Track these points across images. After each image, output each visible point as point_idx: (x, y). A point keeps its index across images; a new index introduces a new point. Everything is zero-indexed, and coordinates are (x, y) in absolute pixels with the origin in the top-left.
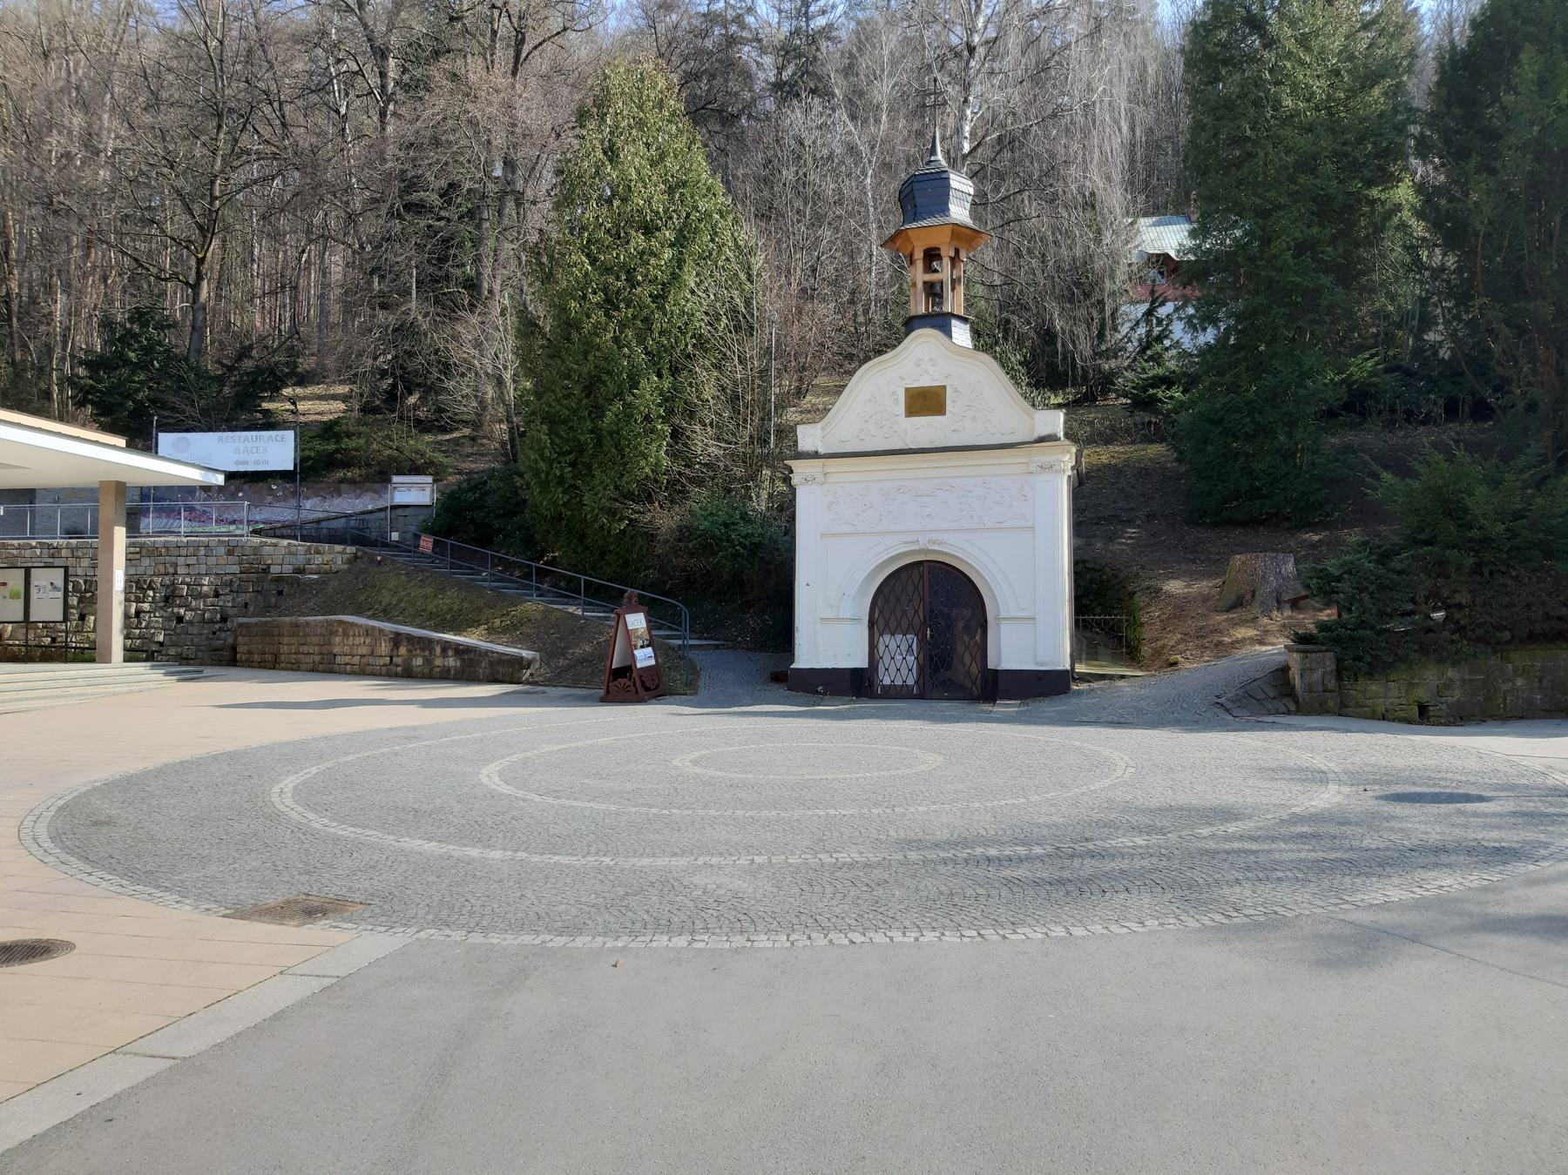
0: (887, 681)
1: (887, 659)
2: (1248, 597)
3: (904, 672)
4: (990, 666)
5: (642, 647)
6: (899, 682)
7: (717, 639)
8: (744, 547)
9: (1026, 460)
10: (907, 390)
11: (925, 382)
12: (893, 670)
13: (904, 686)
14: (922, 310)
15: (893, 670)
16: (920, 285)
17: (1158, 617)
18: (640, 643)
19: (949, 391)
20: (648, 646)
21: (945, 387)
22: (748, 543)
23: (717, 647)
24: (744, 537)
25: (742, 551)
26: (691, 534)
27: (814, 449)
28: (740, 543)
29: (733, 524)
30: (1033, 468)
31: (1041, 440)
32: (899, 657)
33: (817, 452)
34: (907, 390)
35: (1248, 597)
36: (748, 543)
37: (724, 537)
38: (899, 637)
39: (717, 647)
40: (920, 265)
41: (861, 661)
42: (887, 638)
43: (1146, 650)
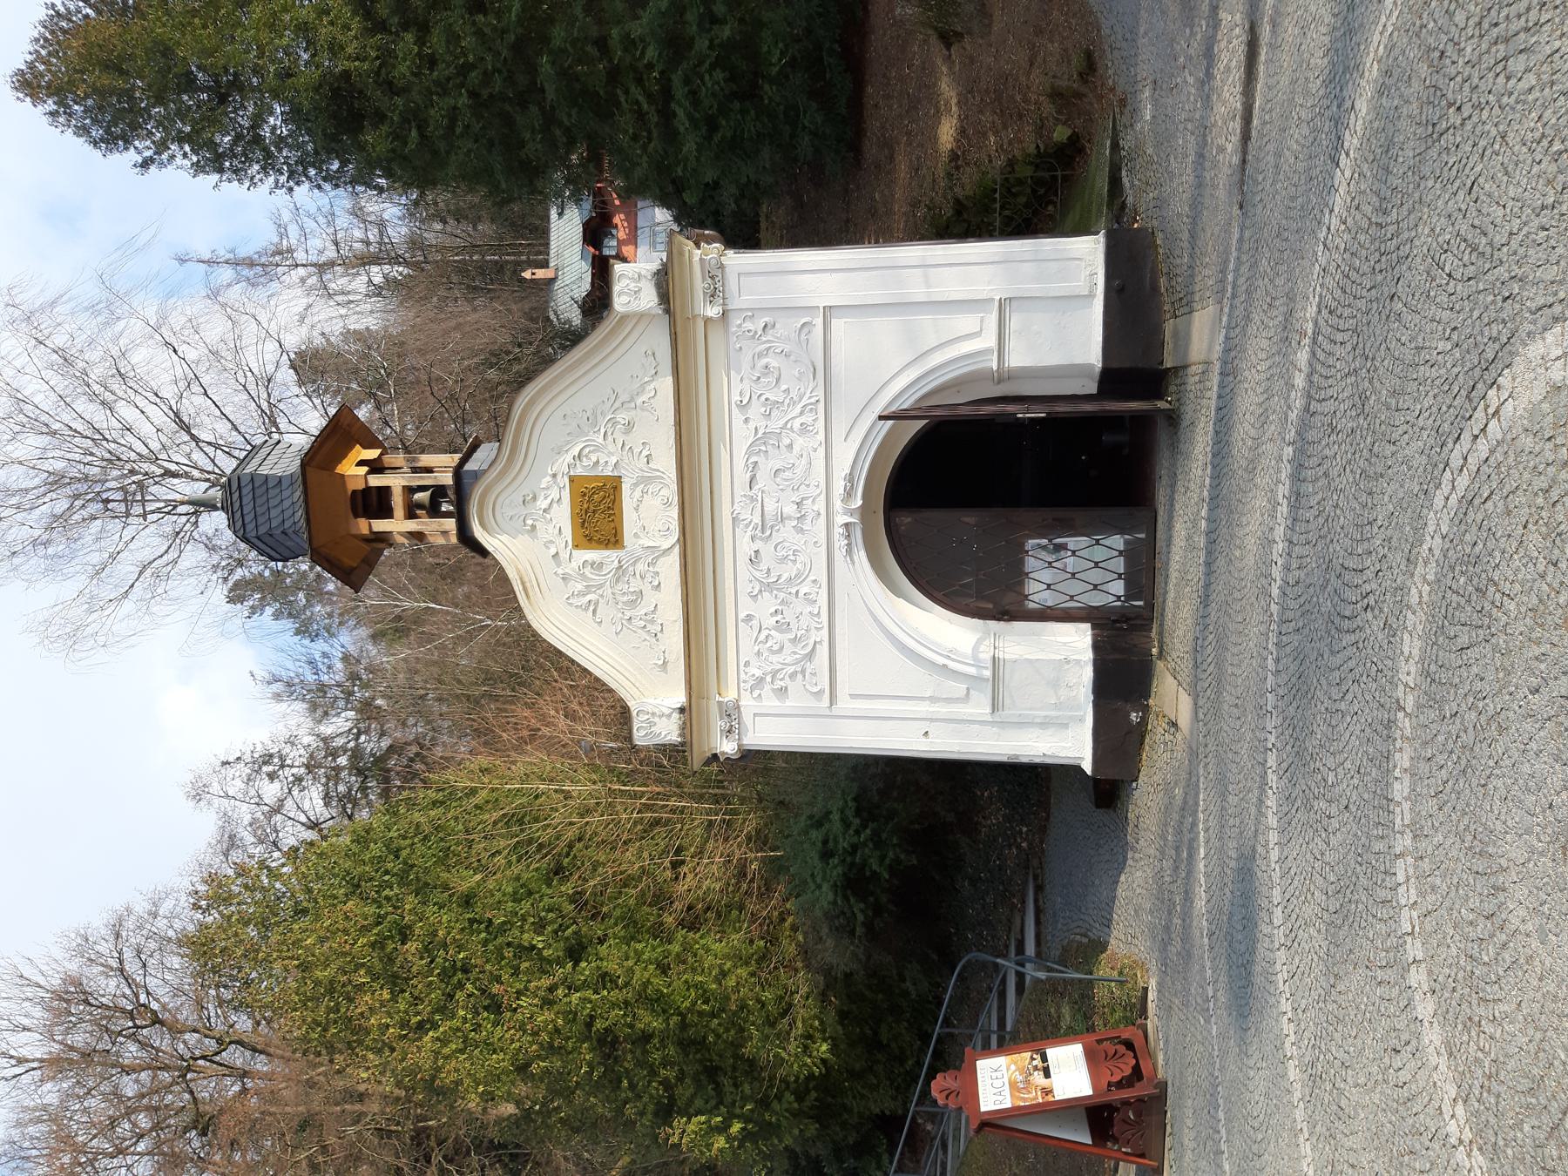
0: (1118, 587)
1: (1075, 587)
3: (1099, 553)
5: (1047, 1074)
6: (1119, 565)
7: (1025, 883)
9: (701, 324)
12: (1095, 576)
13: (1129, 554)
14: (450, 524)
15: (1095, 576)
16: (412, 526)
17: (996, 133)
18: (1038, 1078)
19: (579, 471)
20: (1044, 1059)
21: (572, 480)
23: (1039, 889)
25: (868, 831)
26: (843, 913)
27: (676, 715)
28: (857, 832)
29: (825, 842)
30: (713, 311)
31: (665, 297)
33: (682, 710)
34: (576, 546)
37: (849, 859)
39: (1039, 889)
40: (380, 525)
41: (1077, 641)
42: (1032, 587)
43: (1061, 134)
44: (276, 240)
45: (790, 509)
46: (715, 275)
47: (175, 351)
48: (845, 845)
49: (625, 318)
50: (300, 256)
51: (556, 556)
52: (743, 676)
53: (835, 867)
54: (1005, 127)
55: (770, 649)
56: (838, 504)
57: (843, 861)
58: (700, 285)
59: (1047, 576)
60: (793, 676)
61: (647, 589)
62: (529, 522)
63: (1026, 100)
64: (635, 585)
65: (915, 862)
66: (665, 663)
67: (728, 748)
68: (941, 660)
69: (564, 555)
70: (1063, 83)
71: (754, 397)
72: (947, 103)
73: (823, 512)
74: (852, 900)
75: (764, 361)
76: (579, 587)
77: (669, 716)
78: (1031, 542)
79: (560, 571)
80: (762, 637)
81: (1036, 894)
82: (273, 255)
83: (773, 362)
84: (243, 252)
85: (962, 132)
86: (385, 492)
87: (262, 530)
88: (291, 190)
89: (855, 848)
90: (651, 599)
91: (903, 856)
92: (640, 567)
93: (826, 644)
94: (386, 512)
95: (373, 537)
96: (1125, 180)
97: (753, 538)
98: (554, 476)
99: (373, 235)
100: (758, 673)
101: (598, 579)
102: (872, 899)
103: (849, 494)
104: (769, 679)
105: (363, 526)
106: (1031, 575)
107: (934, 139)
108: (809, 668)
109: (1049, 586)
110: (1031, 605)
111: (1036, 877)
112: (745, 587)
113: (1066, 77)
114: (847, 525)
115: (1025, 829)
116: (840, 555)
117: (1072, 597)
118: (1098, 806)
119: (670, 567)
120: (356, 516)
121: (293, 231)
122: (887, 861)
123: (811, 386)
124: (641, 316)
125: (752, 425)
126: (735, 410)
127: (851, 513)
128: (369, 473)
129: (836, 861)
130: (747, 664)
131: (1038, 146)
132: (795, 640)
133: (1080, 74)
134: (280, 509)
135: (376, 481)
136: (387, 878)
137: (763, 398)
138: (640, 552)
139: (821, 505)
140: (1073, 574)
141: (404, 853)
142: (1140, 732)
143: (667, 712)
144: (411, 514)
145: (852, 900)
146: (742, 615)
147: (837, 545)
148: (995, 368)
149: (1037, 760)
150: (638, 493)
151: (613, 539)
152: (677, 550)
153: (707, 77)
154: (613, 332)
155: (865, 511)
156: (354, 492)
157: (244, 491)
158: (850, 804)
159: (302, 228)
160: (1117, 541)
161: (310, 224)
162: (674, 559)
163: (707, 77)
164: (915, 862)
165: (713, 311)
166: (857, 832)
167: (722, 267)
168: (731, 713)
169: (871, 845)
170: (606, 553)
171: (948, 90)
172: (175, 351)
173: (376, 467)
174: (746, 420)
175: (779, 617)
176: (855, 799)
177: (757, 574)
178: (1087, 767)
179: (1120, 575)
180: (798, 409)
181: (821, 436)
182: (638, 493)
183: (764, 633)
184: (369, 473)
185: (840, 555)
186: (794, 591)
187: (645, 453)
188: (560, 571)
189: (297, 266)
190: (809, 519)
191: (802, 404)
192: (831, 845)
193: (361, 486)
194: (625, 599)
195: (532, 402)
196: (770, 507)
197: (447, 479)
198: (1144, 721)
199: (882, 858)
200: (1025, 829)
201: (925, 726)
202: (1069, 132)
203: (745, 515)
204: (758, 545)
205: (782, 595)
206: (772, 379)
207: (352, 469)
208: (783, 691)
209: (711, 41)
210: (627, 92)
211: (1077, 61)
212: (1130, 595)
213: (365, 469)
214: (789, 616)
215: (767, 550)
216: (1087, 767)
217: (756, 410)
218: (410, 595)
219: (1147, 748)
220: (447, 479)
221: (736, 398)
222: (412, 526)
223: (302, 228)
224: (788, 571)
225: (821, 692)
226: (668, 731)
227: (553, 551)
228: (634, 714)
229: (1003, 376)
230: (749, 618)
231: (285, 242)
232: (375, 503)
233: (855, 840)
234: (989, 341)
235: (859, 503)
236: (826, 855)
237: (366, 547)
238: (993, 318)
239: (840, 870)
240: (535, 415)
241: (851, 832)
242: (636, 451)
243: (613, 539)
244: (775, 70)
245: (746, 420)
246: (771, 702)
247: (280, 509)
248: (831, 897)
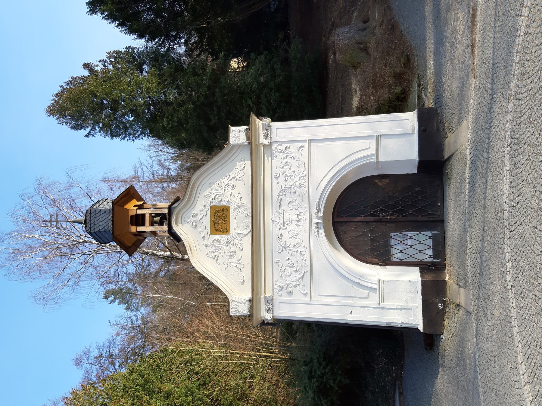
0: (430, 252)
1: (411, 251)
2: (362, 46)
3: (421, 237)
4: (415, 171)
6: (430, 242)
7: (395, 392)
8: (327, 365)
10: (211, 233)
11: (207, 221)
12: (420, 247)
13: (434, 238)
14: (165, 228)
15: (420, 247)
16: (152, 229)
17: (374, 96)
19: (214, 204)
21: (211, 207)
22: (324, 363)
23: (401, 394)
24: (320, 365)
25: (329, 367)
27: (247, 303)
28: (324, 368)
29: (311, 372)
31: (249, 138)
32: (409, 242)
33: (250, 301)
34: (211, 233)
35: (362, 46)
36: (324, 363)
38: (392, 242)
40: (140, 229)
42: (394, 251)
43: (398, 89)
44: (133, 173)
45: (294, 217)
46: (267, 128)
47: (90, 198)
48: (319, 373)
49: (234, 146)
50: (141, 179)
51: (203, 237)
52: (275, 286)
53: (314, 383)
54: (377, 92)
55: (286, 275)
56: (314, 215)
57: (318, 381)
58: (261, 132)
59: (400, 247)
60: (295, 286)
61: (238, 250)
62: (194, 224)
63: (384, 80)
64: (234, 248)
65: (348, 382)
66: (244, 281)
67: (268, 317)
68: (357, 281)
69: (207, 237)
70: (398, 70)
71: (281, 174)
72: (355, 90)
73: (308, 218)
74: (321, 398)
75: (285, 160)
76: (212, 250)
77: (245, 303)
78: (392, 234)
79: (205, 243)
80: (283, 269)
81: (400, 396)
82: (132, 179)
83: (288, 160)
84: (123, 178)
85: (361, 99)
86: (143, 215)
87: (97, 230)
88: (133, 140)
89: (323, 374)
90: (239, 254)
91: (343, 380)
92: (236, 241)
93: (309, 273)
94: (143, 225)
95: (137, 233)
96: (424, 96)
97: (280, 229)
98: (205, 206)
99: (165, 171)
100: (281, 285)
101: (219, 246)
102: (330, 398)
103: (318, 211)
104: (285, 287)
105: (133, 229)
106: (393, 256)
107: (351, 104)
108: (302, 283)
109: (401, 251)
110: (394, 260)
111: (399, 388)
112: (276, 249)
113: (399, 67)
114: (317, 223)
115: (394, 368)
116: (314, 236)
117: (411, 256)
118: (426, 349)
119: (247, 242)
120: (132, 225)
121: (139, 171)
122: (337, 382)
123: (303, 169)
124: (240, 146)
125: (280, 184)
126: (274, 179)
127: (319, 218)
128: (138, 209)
129: (315, 380)
130: (276, 281)
131: (389, 97)
132: (296, 271)
133: (404, 64)
134: (104, 222)
135: (140, 212)
136: (138, 387)
137: (285, 174)
138: (236, 235)
139: (306, 216)
140: (411, 246)
141: (146, 376)
142: (443, 312)
143: (244, 301)
144: (152, 224)
145: (321, 398)
146: (275, 260)
147: (313, 231)
148: (376, 161)
149: (399, 325)
150: (236, 212)
151: (226, 230)
152: (250, 235)
153: (273, 95)
154: (229, 151)
155: (324, 218)
156: (132, 216)
157: (92, 215)
158: (321, 356)
159: (142, 170)
160: (429, 233)
161: (145, 169)
162: (249, 237)
163: (273, 95)
164: (348, 382)
165: (266, 142)
166: (324, 368)
167: (270, 126)
168: (270, 301)
169: (330, 374)
170: (223, 236)
171: (355, 87)
172: (90, 198)
173: (140, 207)
174: (278, 183)
175: (290, 261)
176: (323, 354)
177: (282, 244)
178: (421, 328)
179: (430, 246)
180: (298, 179)
181: (307, 189)
182: (236, 212)
183: (284, 268)
184: (138, 209)
185: (314, 236)
186: (296, 250)
187: (239, 197)
188: (205, 243)
189: (140, 182)
190: (302, 221)
191: (299, 176)
192: (313, 373)
193: (134, 213)
194: (229, 254)
195: (198, 178)
196: (287, 217)
197: (166, 211)
198: (444, 307)
199: (334, 380)
200: (394, 368)
201: (351, 309)
202: (401, 89)
203: (277, 220)
204: (281, 231)
205: (291, 252)
206: (288, 167)
207: (132, 207)
208: (291, 293)
209: (274, 83)
210: (246, 101)
211: (403, 60)
212: (435, 256)
213: (137, 207)
214: (294, 261)
215: (285, 233)
216: (421, 328)
217: (282, 179)
218: (166, 293)
219: (446, 319)
220: (166, 211)
221: (274, 174)
222: (152, 229)
223: (142, 170)
224: (293, 242)
225: (305, 295)
226: (244, 310)
227: (203, 235)
228: (231, 302)
229: (378, 164)
230: (277, 262)
231: (136, 174)
232: (139, 220)
233: (323, 371)
234: (373, 151)
235: (322, 214)
236: (310, 378)
237: (135, 239)
238: (374, 142)
239: (316, 384)
240: (199, 183)
241: (322, 367)
242: (236, 196)
243: (226, 230)
244: (296, 93)
245: (278, 183)
246: (286, 298)
247: (104, 222)
248: (312, 396)
